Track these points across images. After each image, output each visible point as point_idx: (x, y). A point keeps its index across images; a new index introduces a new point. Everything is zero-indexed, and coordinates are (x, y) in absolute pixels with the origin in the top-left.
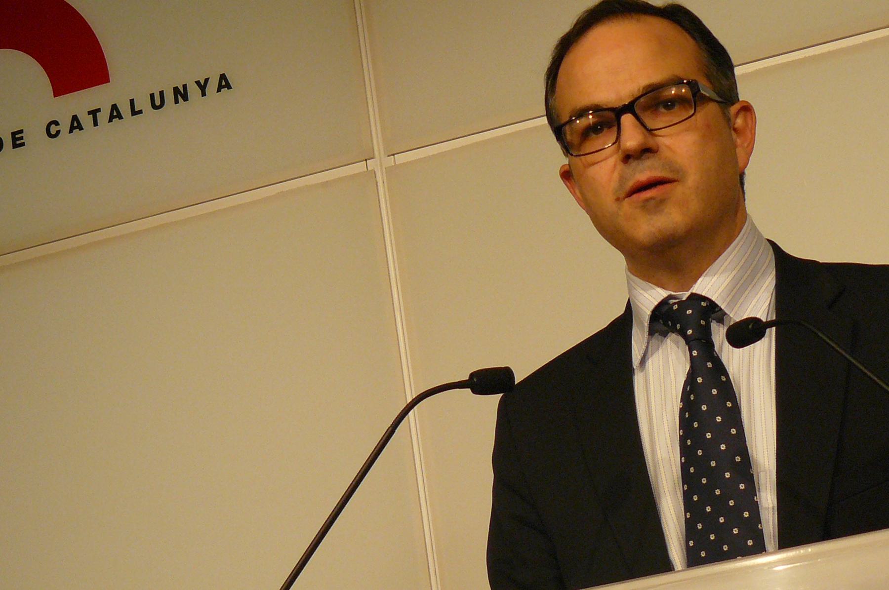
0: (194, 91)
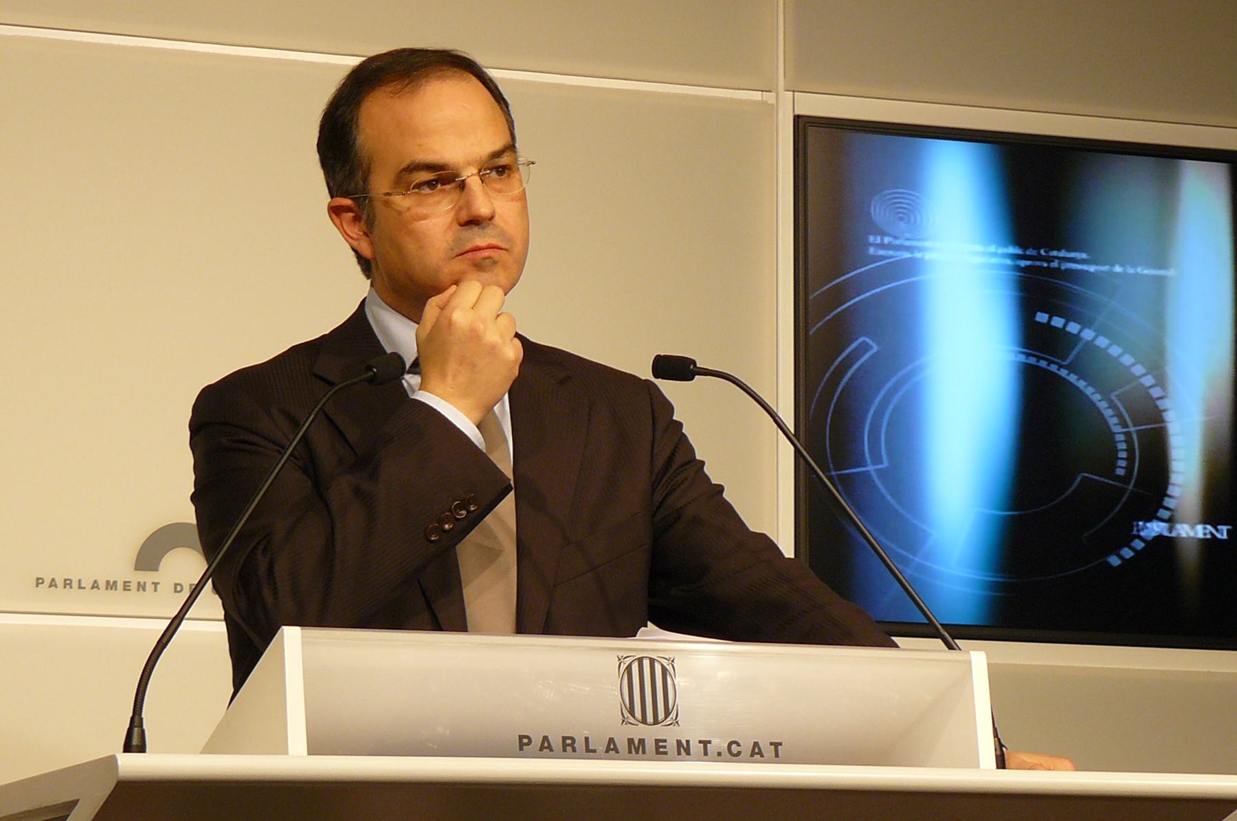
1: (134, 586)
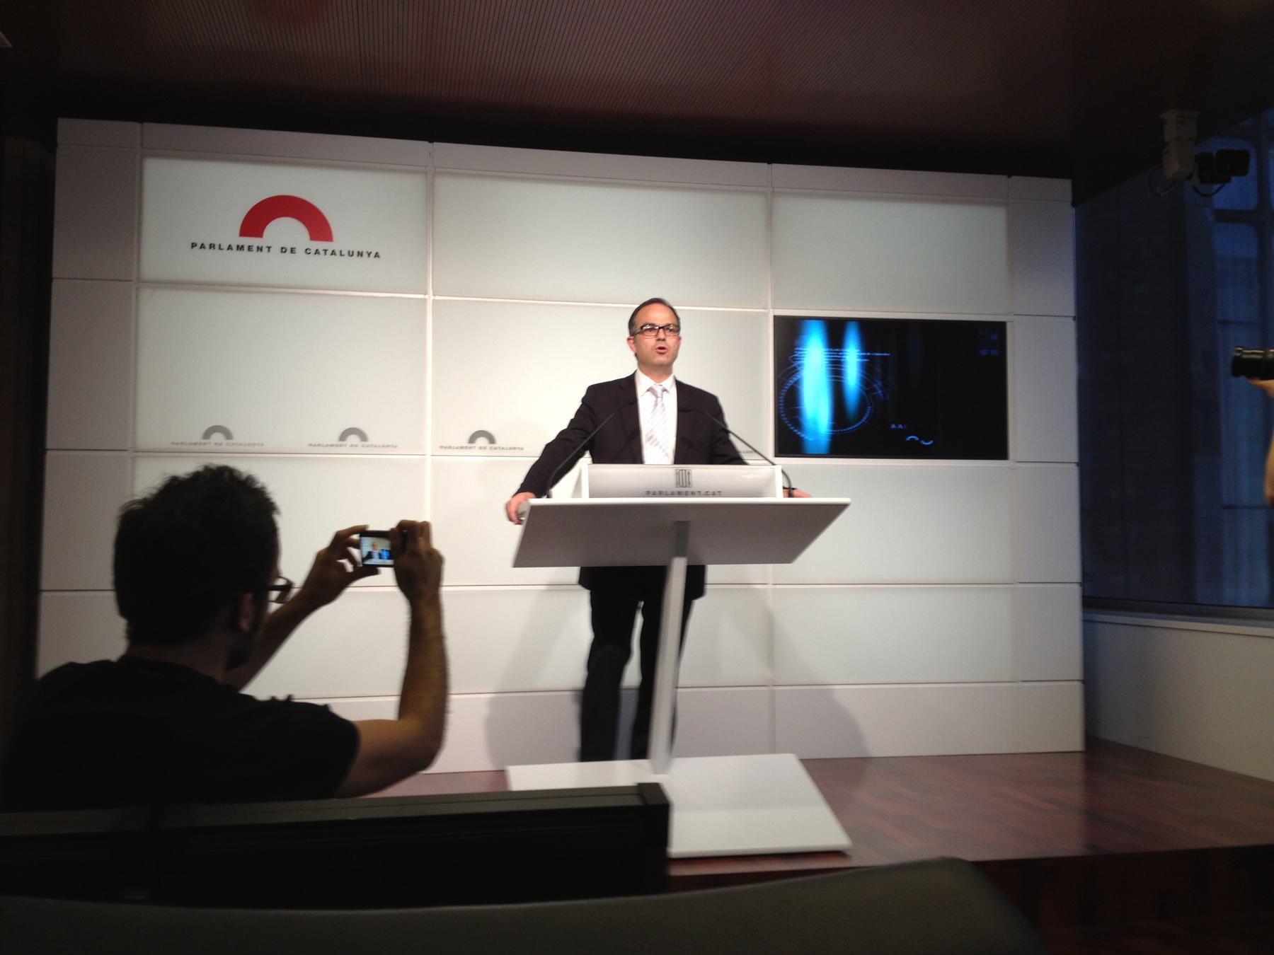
0: (365, 255)
1: (255, 249)
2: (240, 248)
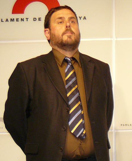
1: (20, 20)
2: (12, 20)
